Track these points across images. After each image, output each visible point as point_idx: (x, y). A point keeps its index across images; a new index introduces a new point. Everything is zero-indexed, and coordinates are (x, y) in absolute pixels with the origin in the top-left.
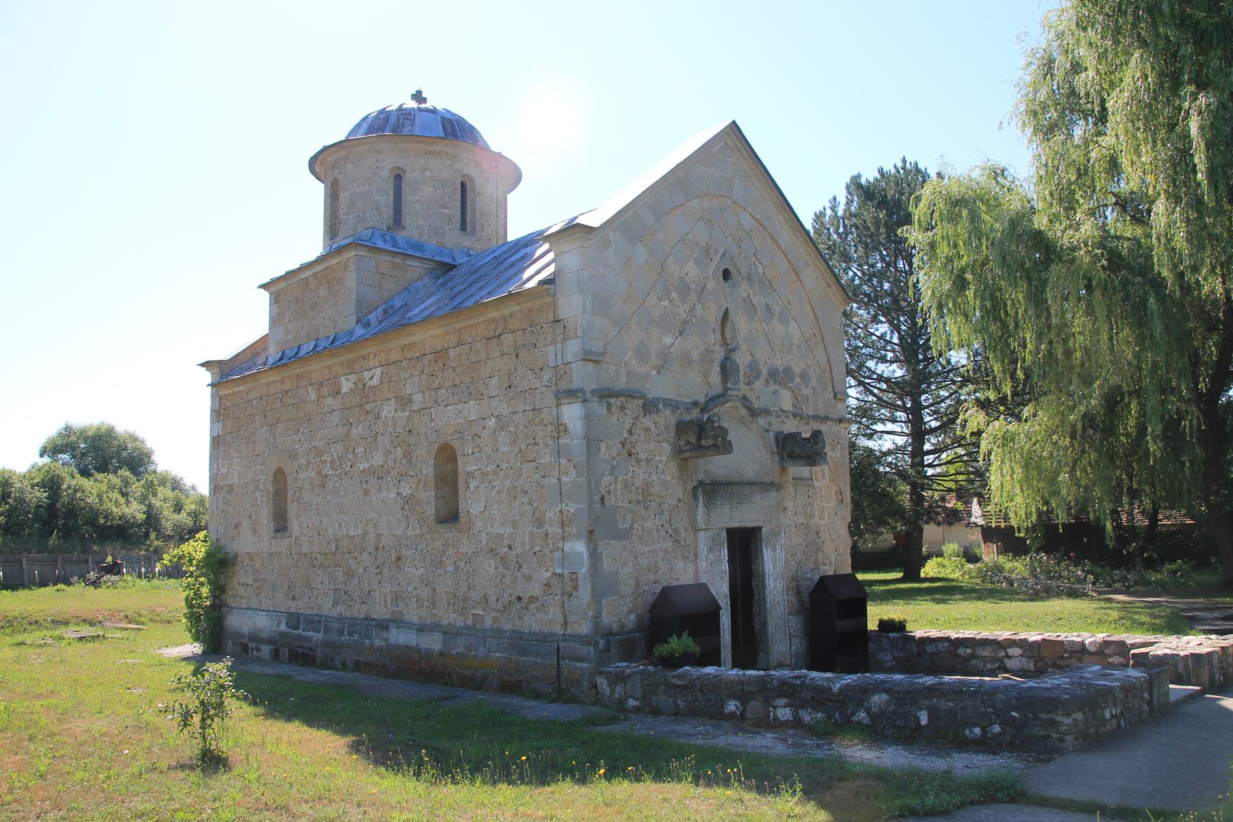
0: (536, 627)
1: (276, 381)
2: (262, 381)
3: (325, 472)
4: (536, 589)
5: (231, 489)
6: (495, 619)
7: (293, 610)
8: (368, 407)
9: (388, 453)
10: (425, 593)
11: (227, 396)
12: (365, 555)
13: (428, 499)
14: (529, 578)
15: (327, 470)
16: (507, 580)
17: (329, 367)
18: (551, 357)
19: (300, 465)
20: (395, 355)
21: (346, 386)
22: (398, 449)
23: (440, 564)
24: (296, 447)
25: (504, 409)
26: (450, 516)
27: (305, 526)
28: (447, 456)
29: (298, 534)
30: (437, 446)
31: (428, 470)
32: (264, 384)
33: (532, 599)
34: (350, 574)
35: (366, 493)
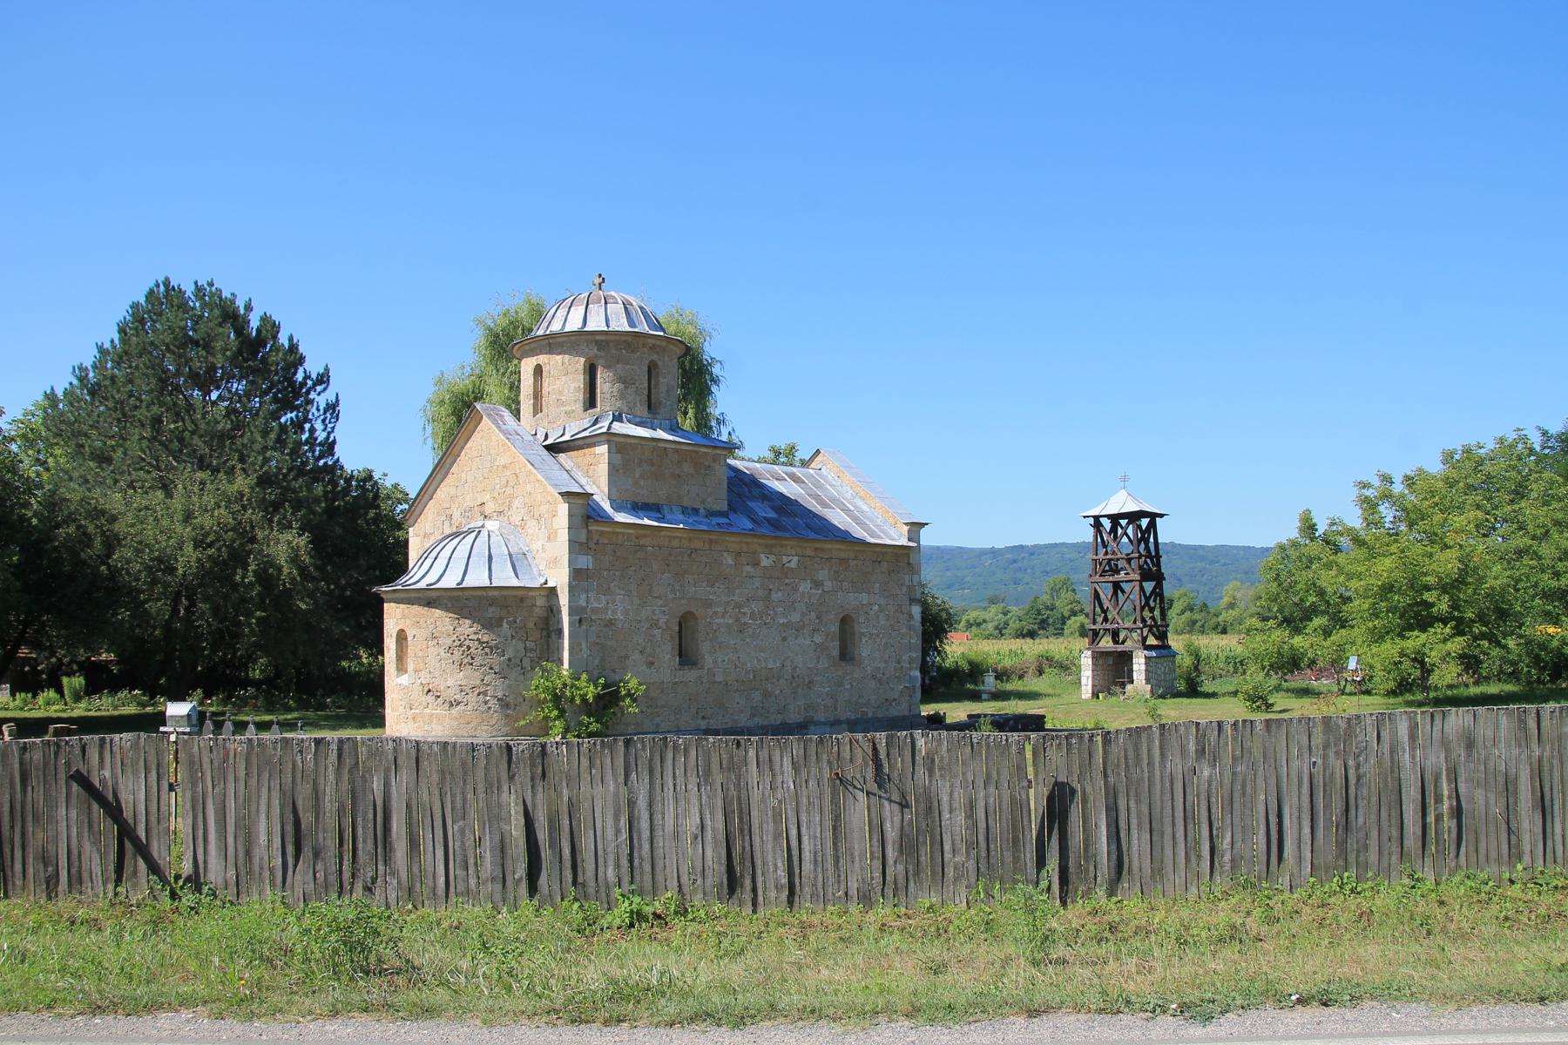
0: (896, 713)
1: (681, 538)
2: (663, 533)
3: (743, 620)
4: (896, 695)
5: (610, 623)
6: (874, 712)
7: (704, 728)
8: (787, 581)
9: (803, 614)
10: (830, 702)
11: (602, 533)
12: (782, 681)
13: (834, 646)
14: (892, 689)
15: (747, 620)
16: (881, 691)
17: (747, 543)
18: (907, 581)
19: (716, 613)
20: (809, 552)
21: (765, 561)
22: (813, 613)
23: (841, 684)
24: (711, 597)
25: (882, 602)
26: (846, 655)
27: (720, 660)
28: (846, 622)
29: (712, 666)
30: (841, 616)
31: (835, 628)
32: (664, 536)
33: (895, 700)
34: (766, 694)
35: (784, 639)
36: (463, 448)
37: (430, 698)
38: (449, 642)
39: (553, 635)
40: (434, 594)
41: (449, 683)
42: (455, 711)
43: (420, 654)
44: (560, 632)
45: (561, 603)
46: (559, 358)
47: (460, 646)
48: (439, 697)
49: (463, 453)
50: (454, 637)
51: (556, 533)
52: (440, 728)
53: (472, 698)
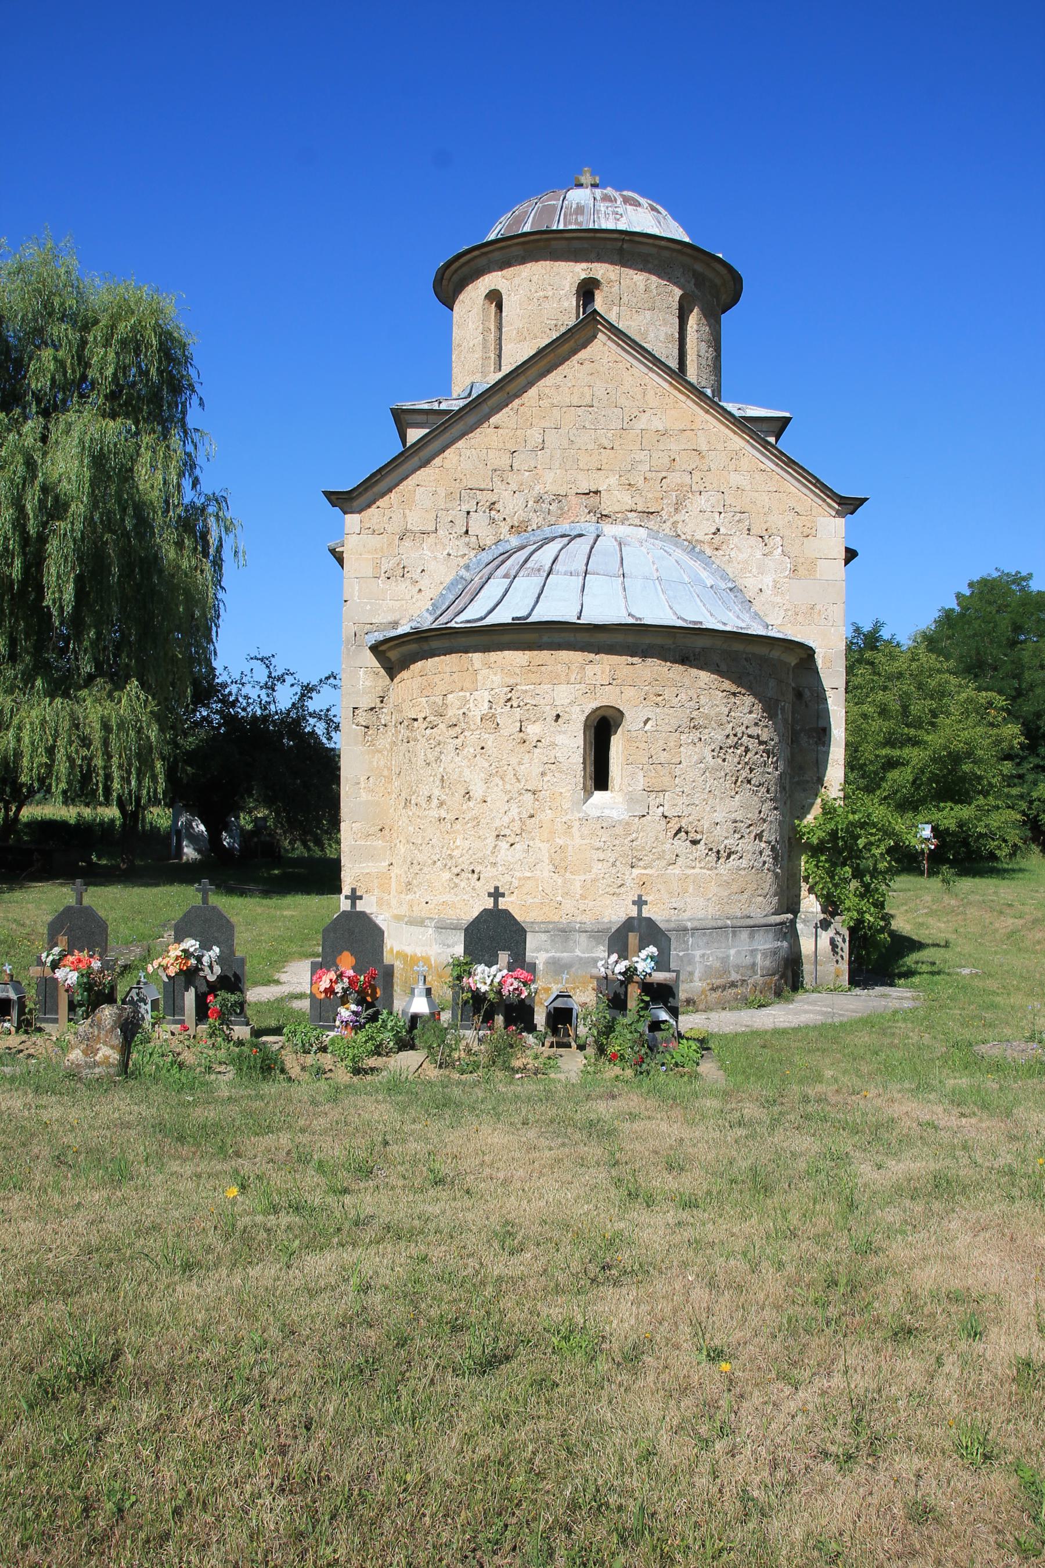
36: (531, 384)
37: (681, 845)
38: (719, 736)
39: (804, 740)
40: (701, 642)
41: (718, 817)
42: (725, 868)
43: (663, 757)
44: (823, 734)
45: (827, 682)
46: (637, 280)
47: (735, 747)
48: (695, 842)
49: (533, 392)
50: (728, 730)
51: (813, 563)
52: (701, 902)
53: (747, 845)
